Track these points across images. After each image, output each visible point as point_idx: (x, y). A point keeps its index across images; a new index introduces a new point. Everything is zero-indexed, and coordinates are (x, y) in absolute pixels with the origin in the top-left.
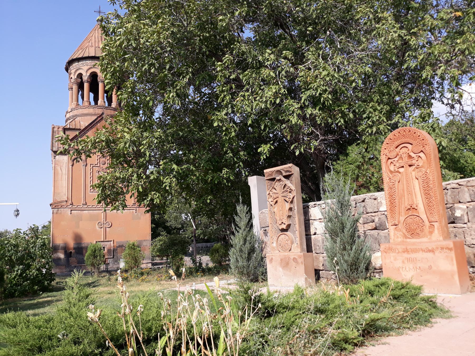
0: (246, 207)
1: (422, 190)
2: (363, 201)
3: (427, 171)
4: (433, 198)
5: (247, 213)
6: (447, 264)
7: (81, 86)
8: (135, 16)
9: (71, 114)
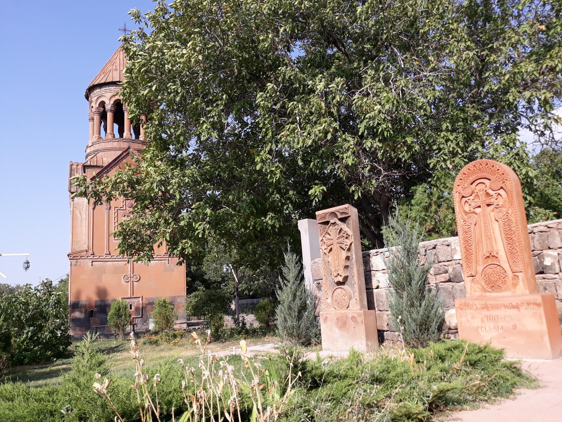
0: (295, 255)
2: (434, 248)
3: (509, 212)
4: (517, 244)
5: (297, 263)
6: (535, 322)
7: (103, 116)
9: (92, 149)
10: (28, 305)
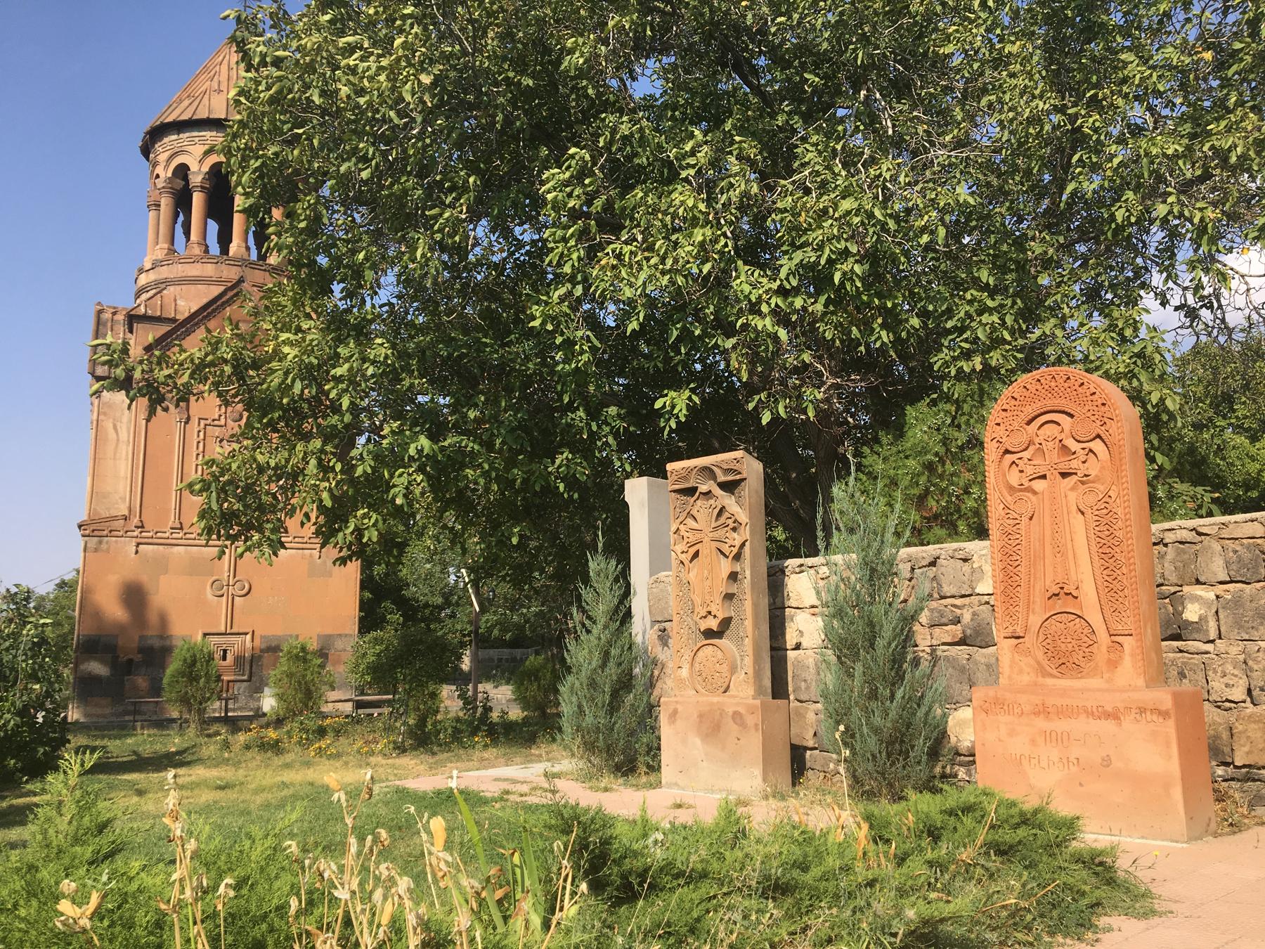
0: (613, 562)
1: (1093, 543)
3: (1111, 493)
4: (1124, 570)
5: (616, 580)
6: (1154, 753)
9: (152, 276)
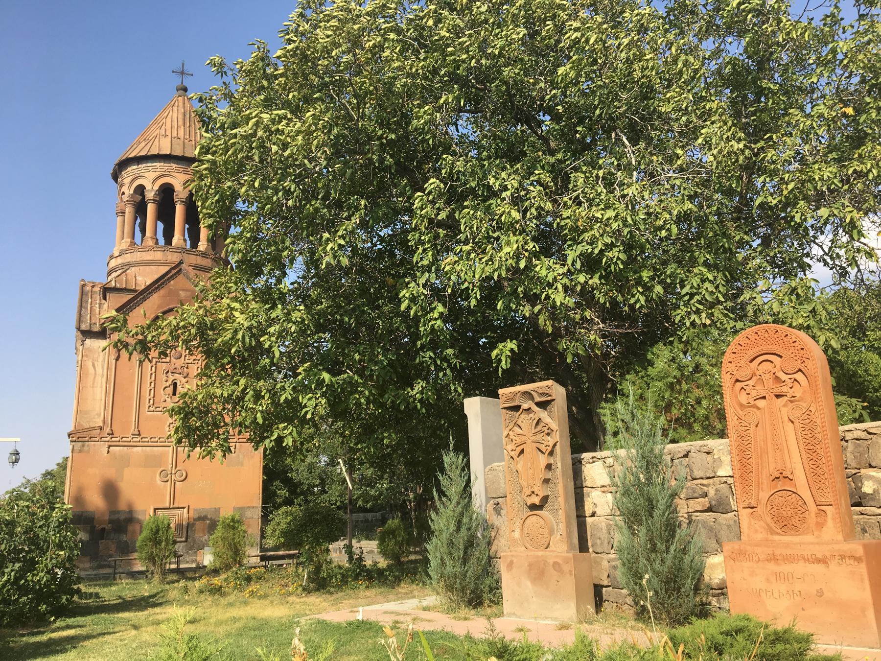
0: (461, 457)
1: (801, 443)
2: (686, 456)
5: (463, 470)
6: (852, 585)
8: (262, 97)
9: (119, 261)
10: (15, 526)
